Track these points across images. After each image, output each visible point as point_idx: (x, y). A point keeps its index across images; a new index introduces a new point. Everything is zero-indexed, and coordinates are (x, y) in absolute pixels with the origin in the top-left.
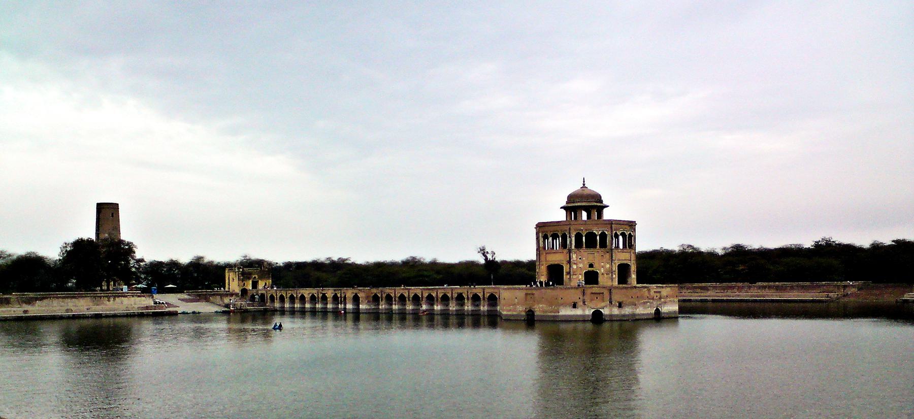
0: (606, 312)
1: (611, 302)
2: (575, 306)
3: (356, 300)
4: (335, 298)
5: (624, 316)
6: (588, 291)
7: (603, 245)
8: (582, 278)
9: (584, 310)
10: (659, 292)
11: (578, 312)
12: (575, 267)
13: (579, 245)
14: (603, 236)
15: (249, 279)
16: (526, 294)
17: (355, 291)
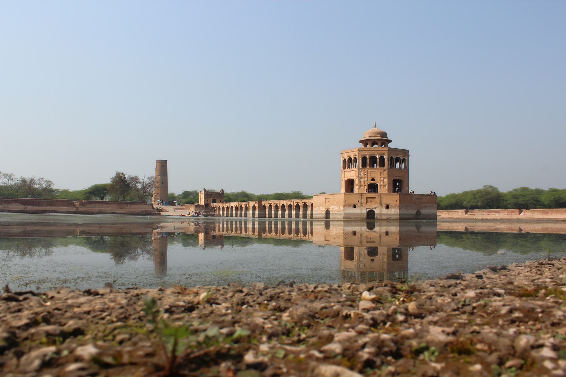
0: (377, 211)
1: (381, 204)
2: (355, 207)
3: (254, 207)
4: (246, 208)
5: (390, 215)
6: (365, 197)
7: (382, 165)
8: (366, 188)
9: (361, 210)
10: (421, 199)
11: (357, 211)
12: (362, 180)
13: (364, 165)
14: (382, 159)
15: (211, 197)
16: (326, 199)
17: (254, 203)
